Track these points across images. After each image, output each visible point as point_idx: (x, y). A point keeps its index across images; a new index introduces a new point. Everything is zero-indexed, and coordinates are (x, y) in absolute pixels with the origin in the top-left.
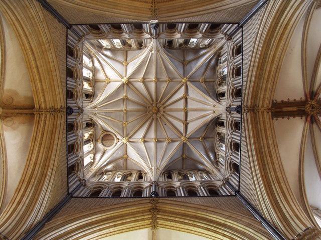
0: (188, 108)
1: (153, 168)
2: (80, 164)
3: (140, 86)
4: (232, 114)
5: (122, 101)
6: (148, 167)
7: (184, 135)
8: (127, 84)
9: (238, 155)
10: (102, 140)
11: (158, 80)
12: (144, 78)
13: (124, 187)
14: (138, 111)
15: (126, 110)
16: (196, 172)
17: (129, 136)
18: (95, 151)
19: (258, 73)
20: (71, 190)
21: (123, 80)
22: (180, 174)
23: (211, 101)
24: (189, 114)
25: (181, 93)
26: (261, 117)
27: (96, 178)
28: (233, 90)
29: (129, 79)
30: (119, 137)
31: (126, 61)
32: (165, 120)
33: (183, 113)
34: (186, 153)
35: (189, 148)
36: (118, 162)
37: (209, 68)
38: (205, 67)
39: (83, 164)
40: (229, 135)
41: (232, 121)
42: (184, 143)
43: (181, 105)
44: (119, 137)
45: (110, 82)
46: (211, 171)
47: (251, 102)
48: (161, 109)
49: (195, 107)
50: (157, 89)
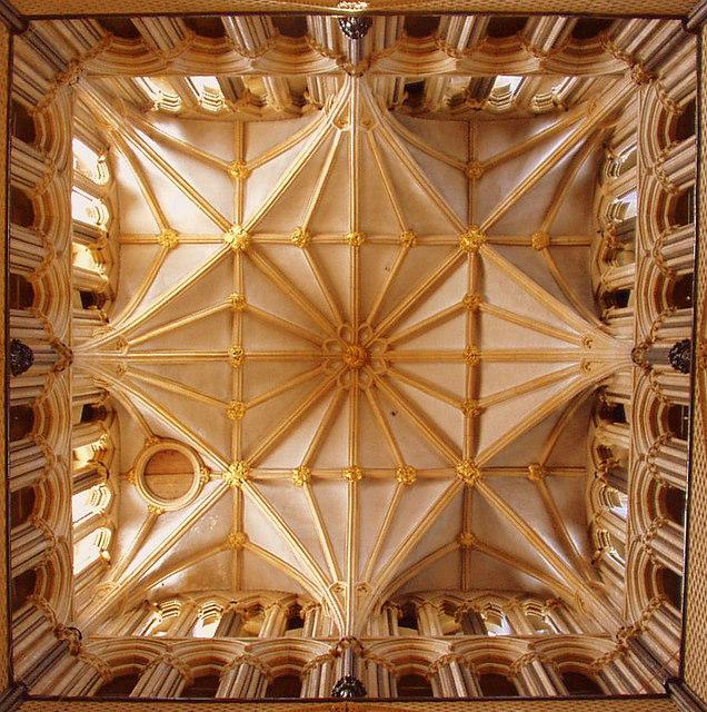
0: (484, 347)
1: (345, 585)
2: (57, 569)
3: (297, 260)
4: (657, 374)
5: (225, 318)
6: (327, 580)
7: (467, 455)
8: (245, 253)
9: (677, 534)
11: (366, 239)
12: (311, 231)
13: (230, 659)
14: (286, 359)
16: (513, 600)
17: (253, 457)
18: (117, 517)
20: (20, 670)
21: (228, 238)
22: (448, 609)
23: (575, 323)
24: (490, 372)
25: (455, 292)
28: (660, 279)
29: (252, 233)
30: (212, 461)
31: (243, 161)
32: (394, 398)
33: (463, 371)
34: (475, 525)
35: (485, 508)
36: (208, 559)
37: (567, 192)
38: (547, 190)
39: (71, 568)
40: (642, 458)
41: (656, 403)
42: (466, 488)
43: (455, 337)
44: (212, 461)
45: (177, 245)
46: (571, 600)
48: (378, 352)
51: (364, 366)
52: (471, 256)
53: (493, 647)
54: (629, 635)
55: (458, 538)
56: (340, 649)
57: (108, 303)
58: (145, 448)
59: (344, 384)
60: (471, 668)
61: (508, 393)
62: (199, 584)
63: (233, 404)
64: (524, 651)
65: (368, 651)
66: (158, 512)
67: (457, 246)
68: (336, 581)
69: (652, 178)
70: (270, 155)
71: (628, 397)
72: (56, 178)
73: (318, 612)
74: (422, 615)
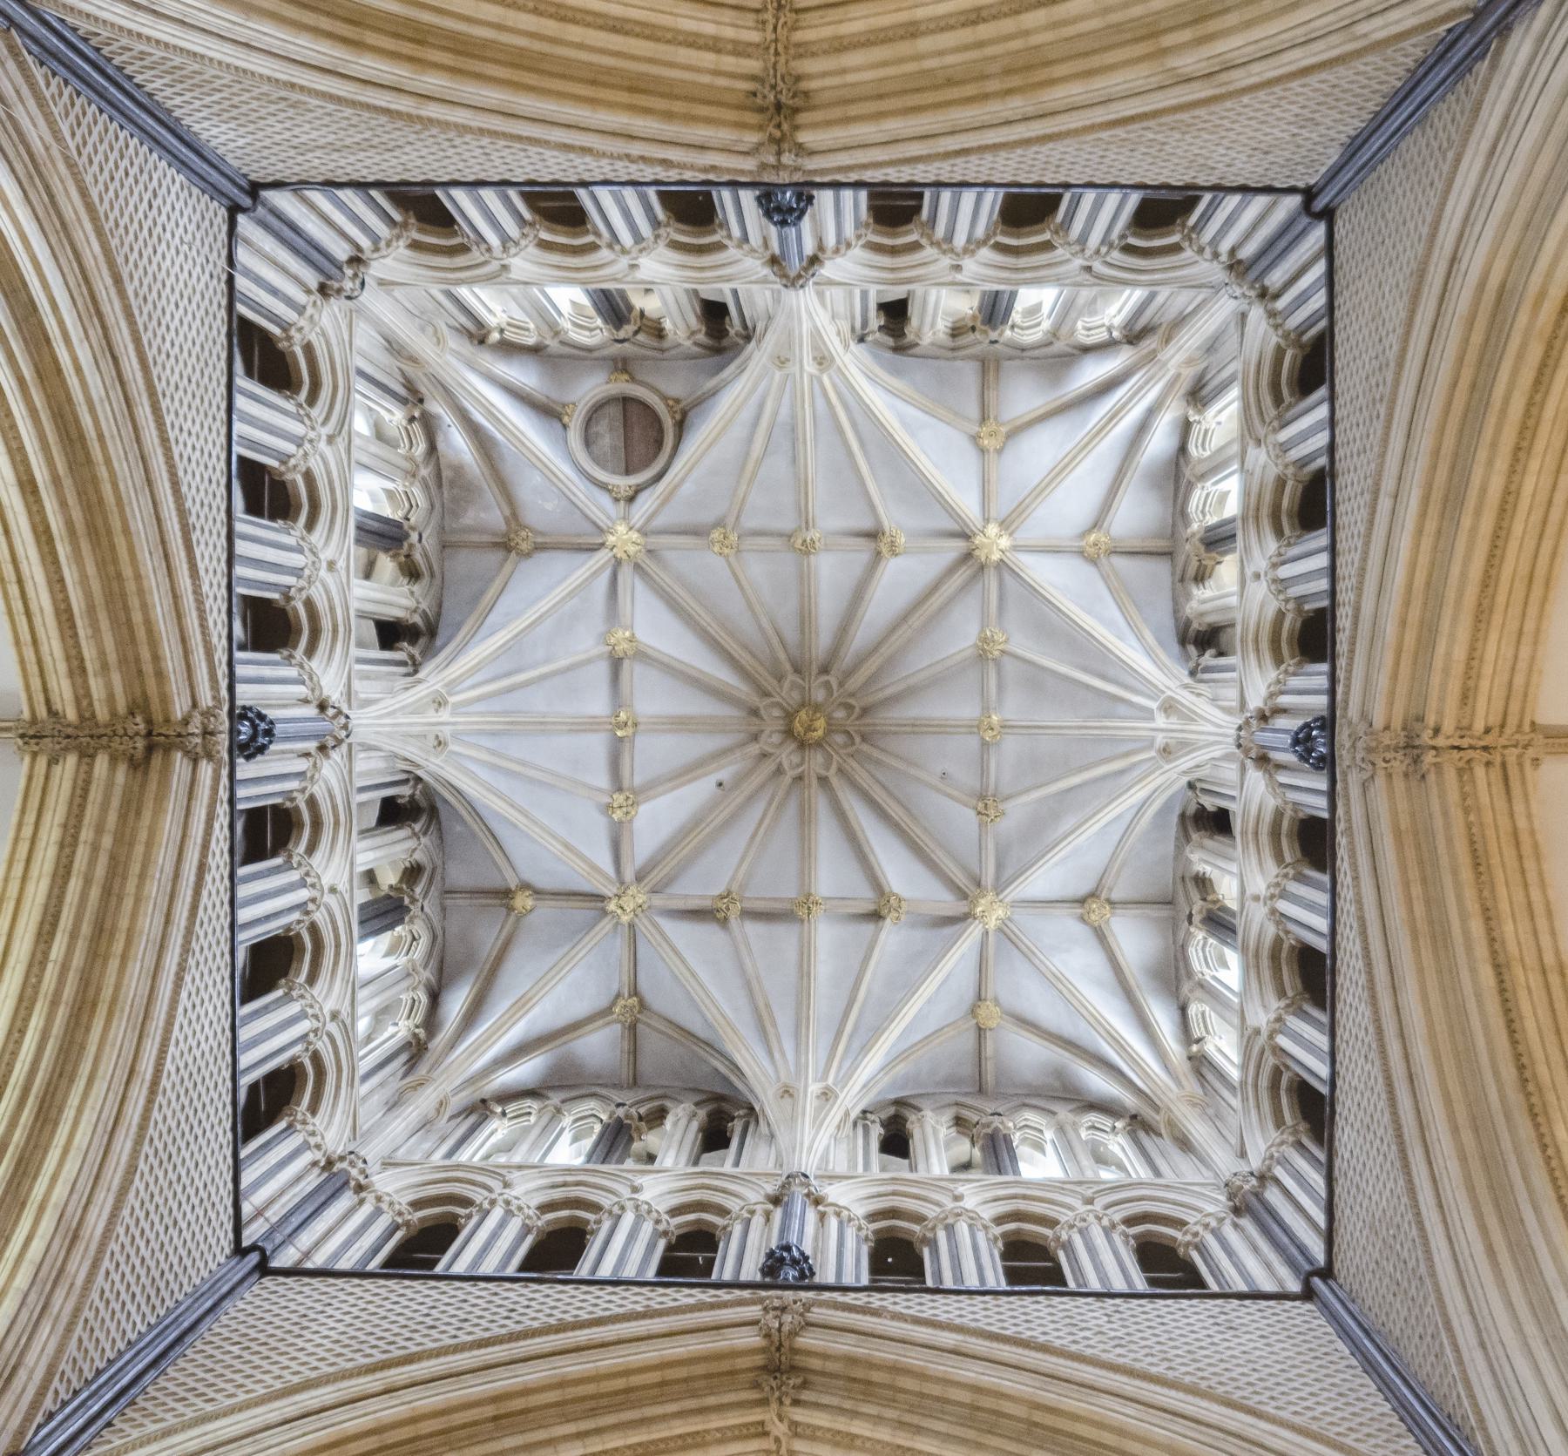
1: (445, 715)
4: (768, 1216)
5: (866, 524)
6: (452, 685)
8: (968, 556)
10: (626, 401)
13: (317, 537)
14: (805, 618)
15: (807, 549)
16: (427, 975)
17: (650, 566)
19: (1008, 1407)
22: (413, 873)
24: (785, 935)
26: (734, 1419)
27: (385, 359)
28: (919, 1218)
30: (646, 502)
31: (1114, 552)
33: (788, 891)
34: (543, 914)
36: (490, 495)
39: (469, 282)
40: (635, 1190)
41: (723, 1211)
42: (601, 898)
45: (983, 451)
46: (422, 1070)
47: (825, 1356)
48: (816, 761)
49: (824, 968)
50: (942, 729)
51: (795, 738)
52: (962, 907)
53: (337, 954)
54: (354, 1172)
55: (525, 886)
56: (331, 712)
57: (890, 341)
58: (664, 398)
59: (765, 707)
60: (299, 922)
61: (747, 961)
62: (452, 484)
63: (733, 538)
64: (328, 1007)
65: (327, 756)
66: (566, 419)
67: (979, 884)
68: (452, 700)
69: (1077, 1203)
70: (1120, 591)
71: (737, 1164)
72: (1079, 262)
73: (402, 670)
74: (402, 833)
